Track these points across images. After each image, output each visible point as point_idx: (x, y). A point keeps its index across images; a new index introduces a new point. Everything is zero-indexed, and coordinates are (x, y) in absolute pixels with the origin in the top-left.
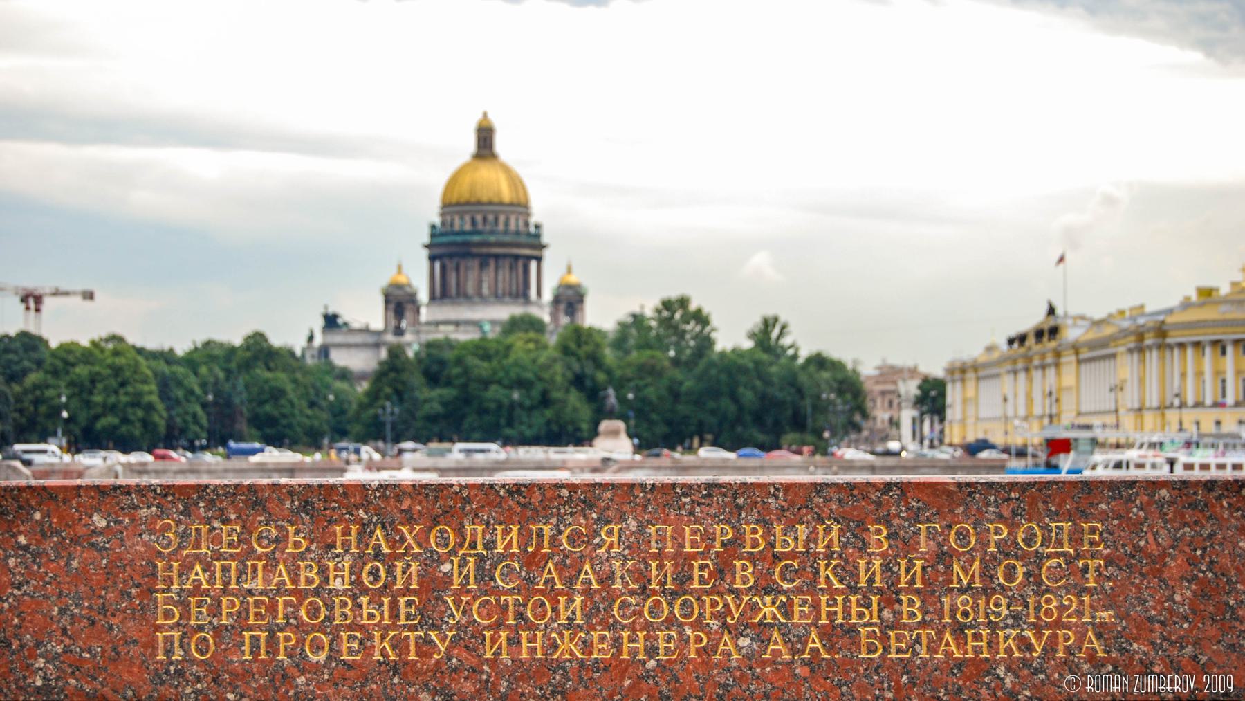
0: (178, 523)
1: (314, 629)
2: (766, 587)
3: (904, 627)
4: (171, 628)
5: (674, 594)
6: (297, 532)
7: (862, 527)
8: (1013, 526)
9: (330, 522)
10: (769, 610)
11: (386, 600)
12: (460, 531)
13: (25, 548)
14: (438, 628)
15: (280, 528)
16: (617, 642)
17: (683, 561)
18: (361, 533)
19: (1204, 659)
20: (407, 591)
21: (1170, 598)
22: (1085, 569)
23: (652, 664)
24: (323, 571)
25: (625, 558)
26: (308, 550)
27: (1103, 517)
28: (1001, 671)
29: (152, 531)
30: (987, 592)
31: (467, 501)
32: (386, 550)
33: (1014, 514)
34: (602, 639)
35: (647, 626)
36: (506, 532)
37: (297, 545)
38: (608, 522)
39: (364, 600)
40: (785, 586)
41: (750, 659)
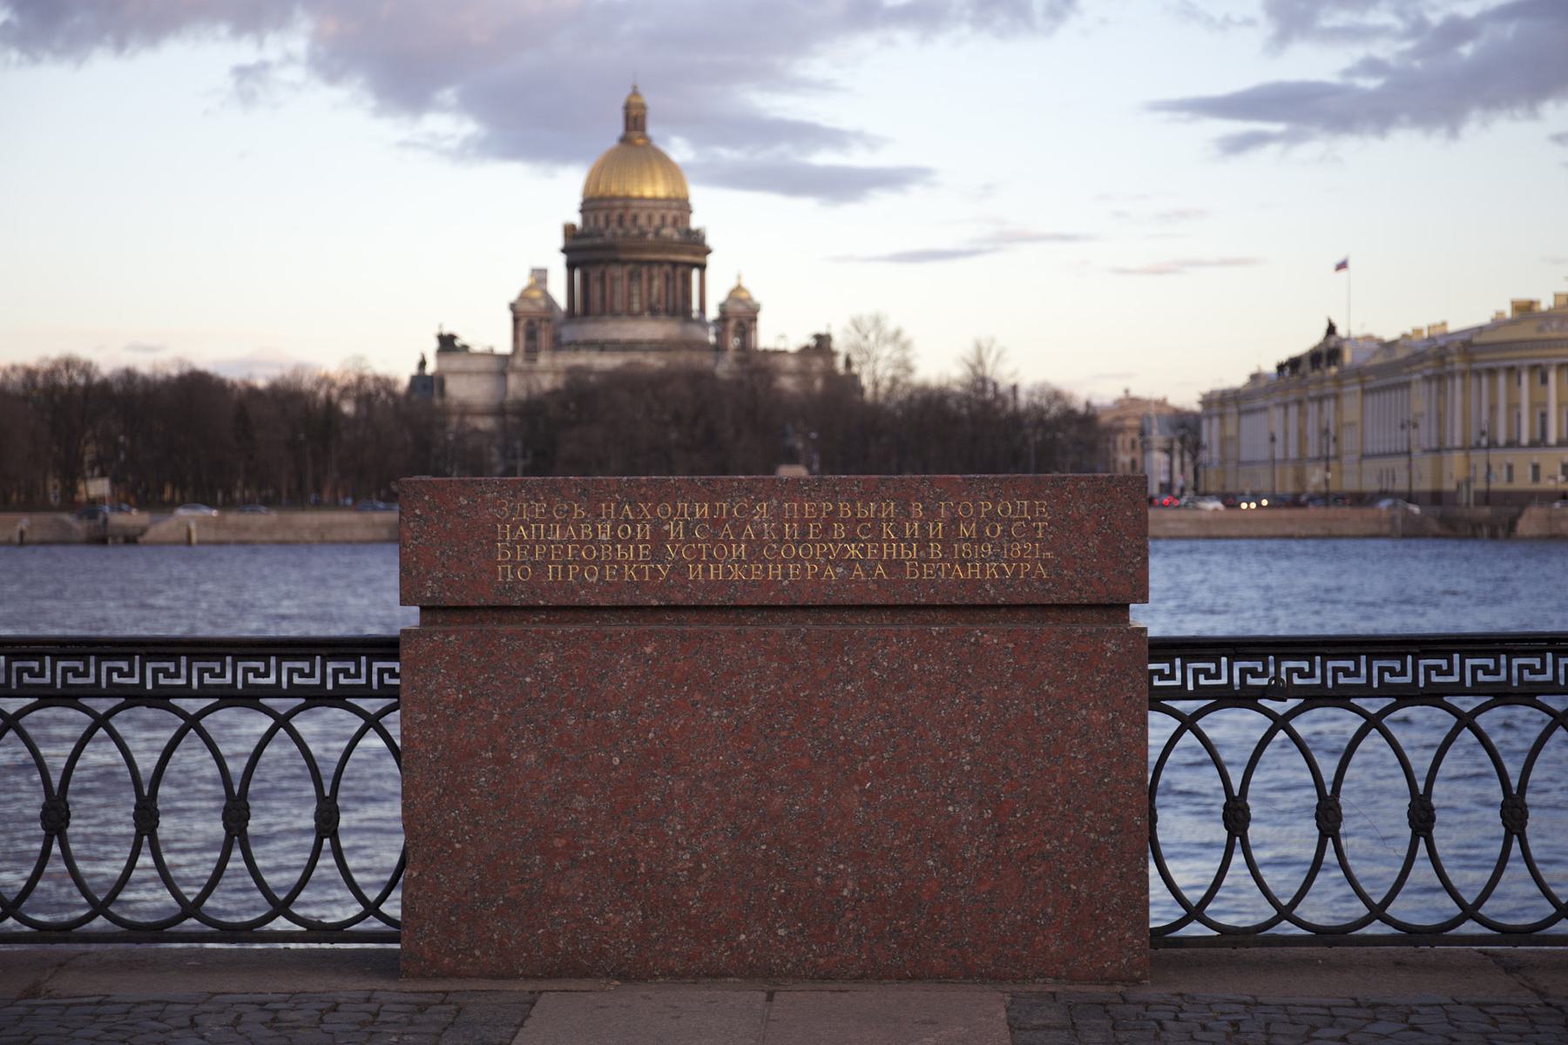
1: (589, 563)
2: (851, 538)
8: (995, 504)
9: (600, 501)
12: (675, 508)
14: (662, 562)
16: (766, 570)
17: (804, 524)
20: (643, 541)
24: (595, 530)
27: (1048, 498)
30: (981, 540)
35: (784, 561)
36: (702, 507)
41: (843, 580)
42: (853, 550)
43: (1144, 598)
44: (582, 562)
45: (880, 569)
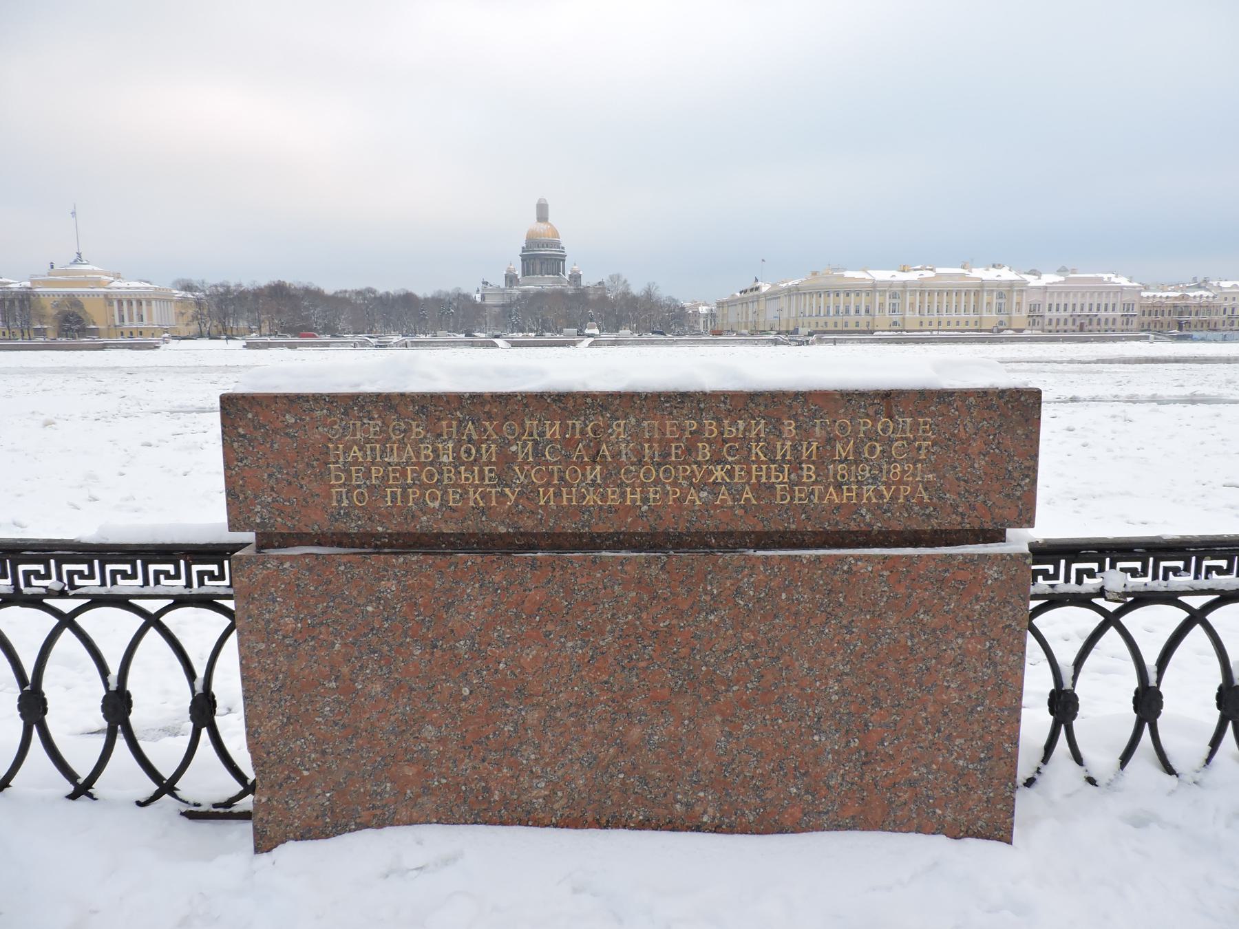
0: (342, 419)
1: (430, 486)
5: (659, 465)
6: (418, 426)
7: (779, 420)
8: (875, 421)
9: (439, 419)
10: (719, 473)
11: (476, 469)
12: (522, 425)
13: (244, 436)
14: (510, 487)
15: (407, 424)
17: (665, 443)
18: (459, 427)
20: (489, 463)
22: (919, 448)
23: (645, 508)
26: (425, 437)
29: (324, 426)
30: (857, 462)
31: (526, 406)
32: (475, 437)
33: (876, 413)
35: (643, 485)
36: (552, 426)
37: (418, 434)
40: (730, 459)
42: (719, 473)
44: (423, 487)
45: (748, 494)
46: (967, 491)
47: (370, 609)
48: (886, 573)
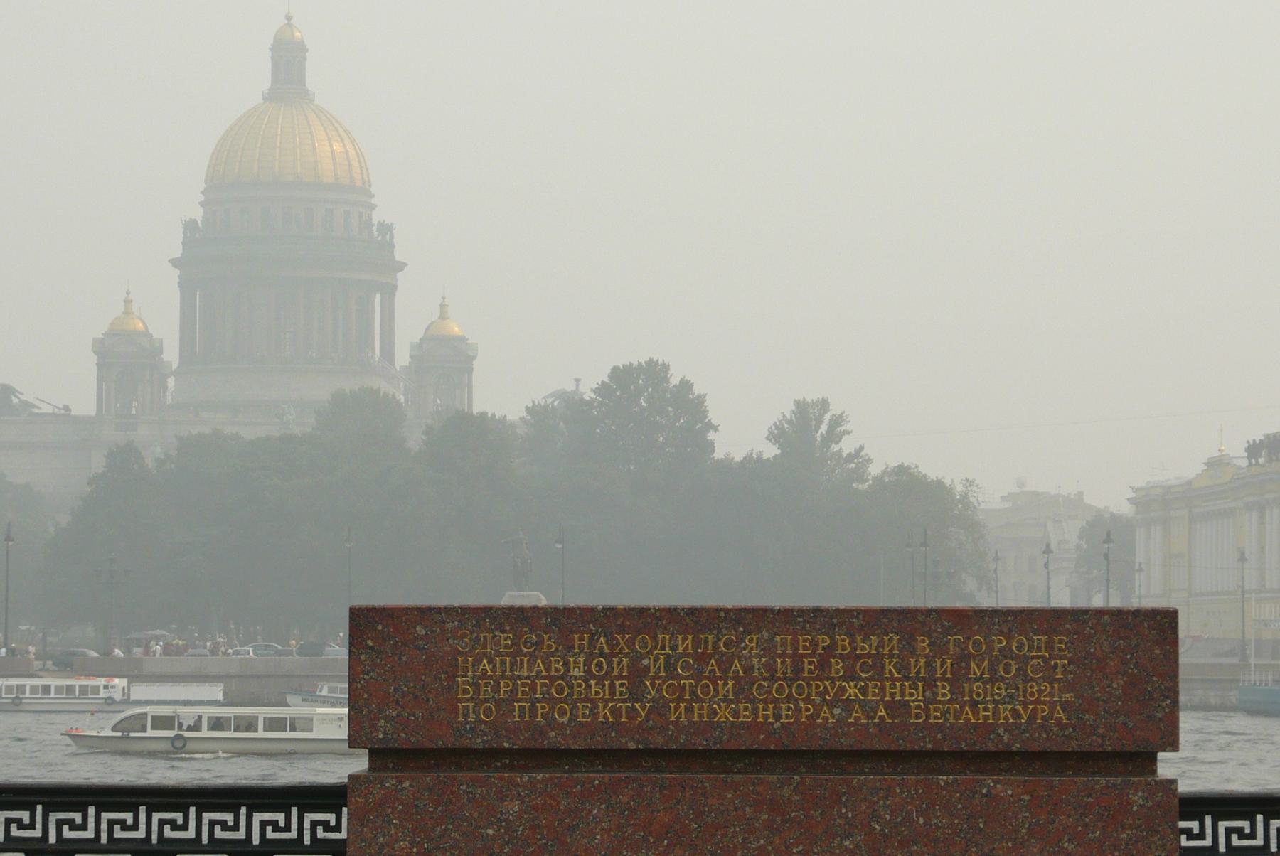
0: (472, 632)
1: (560, 701)
2: (850, 676)
3: (940, 702)
4: (468, 700)
5: (793, 680)
6: (549, 639)
8: (1009, 639)
9: (572, 632)
12: (655, 639)
13: (372, 648)
18: (591, 639)
19: (1131, 725)
20: (620, 677)
21: (1110, 686)
22: (1056, 666)
23: (777, 725)
24: (566, 664)
25: (761, 657)
28: (1001, 731)
29: (455, 637)
30: (993, 680)
31: (659, 619)
32: (607, 651)
33: (1010, 630)
34: (746, 709)
35: (774, 701)
36: (685, 639)
37: (549, 647)
38: (750, 633)
39: (593, 682)
40: (863, 675)
41: (841, 722)
42: (852, 690)
43: (1173, 745)
45: (882, 712)
46: (1106, 712)
47: (490, 832)
48: (1027, 797)
